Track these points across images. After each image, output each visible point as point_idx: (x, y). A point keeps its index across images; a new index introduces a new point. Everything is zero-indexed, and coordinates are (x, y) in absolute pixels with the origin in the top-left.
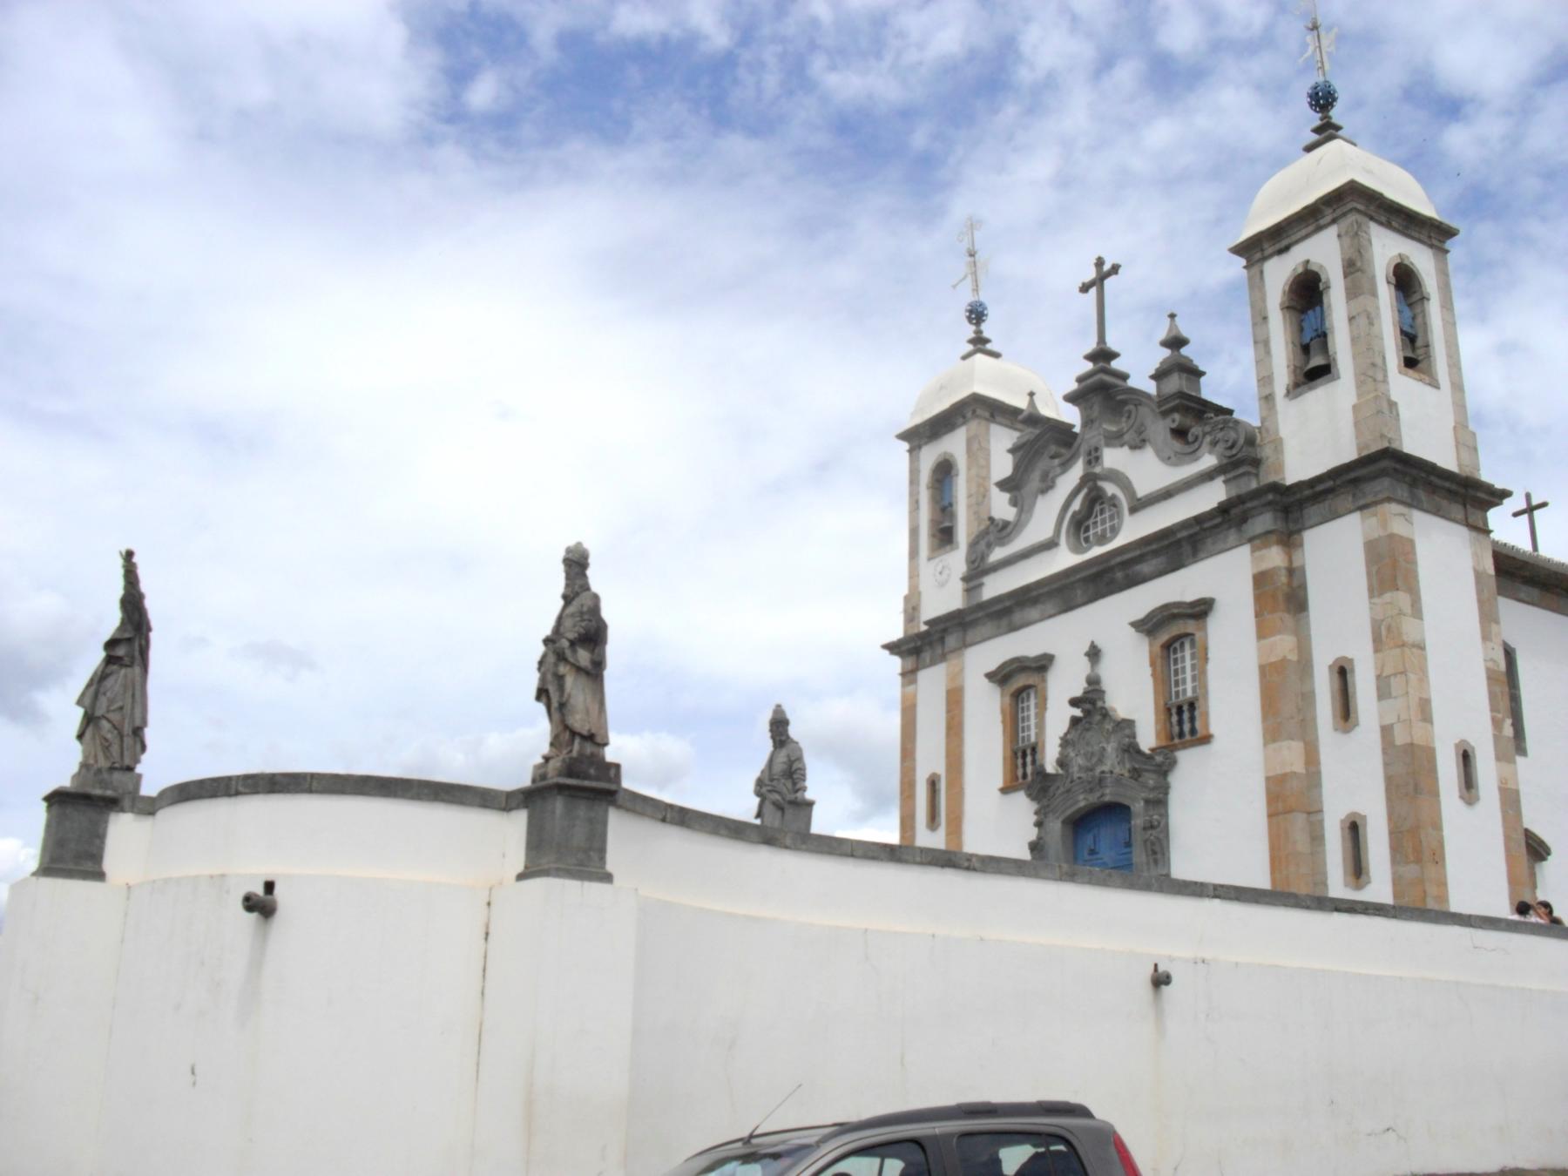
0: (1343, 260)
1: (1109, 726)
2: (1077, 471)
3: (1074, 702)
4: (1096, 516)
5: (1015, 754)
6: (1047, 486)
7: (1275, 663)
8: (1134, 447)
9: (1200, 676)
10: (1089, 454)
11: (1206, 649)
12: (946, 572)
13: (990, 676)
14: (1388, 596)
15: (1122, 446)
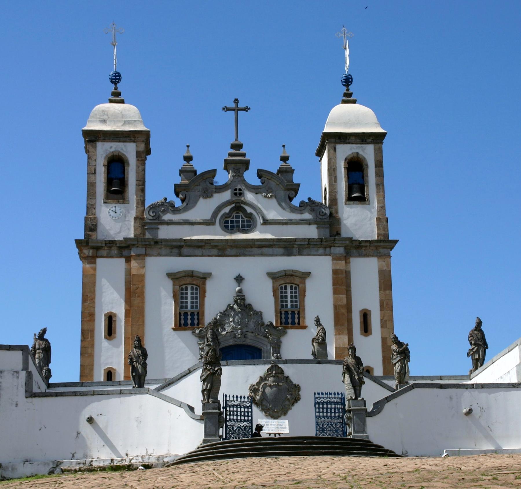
2: (227, 195)
4: (233, 218)
5: (180, 313)
6: (207, 194)
7: (341, 305)
10: (236, 190)
11: (304, 291)
13: (169, 275)
14: (387, 292)
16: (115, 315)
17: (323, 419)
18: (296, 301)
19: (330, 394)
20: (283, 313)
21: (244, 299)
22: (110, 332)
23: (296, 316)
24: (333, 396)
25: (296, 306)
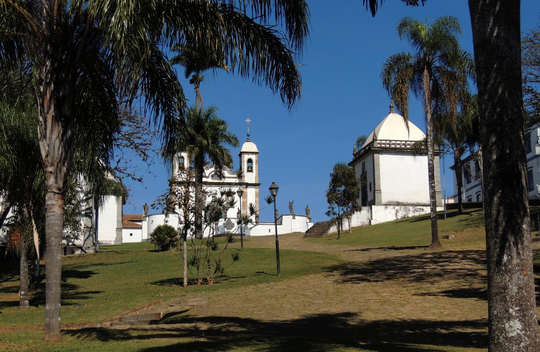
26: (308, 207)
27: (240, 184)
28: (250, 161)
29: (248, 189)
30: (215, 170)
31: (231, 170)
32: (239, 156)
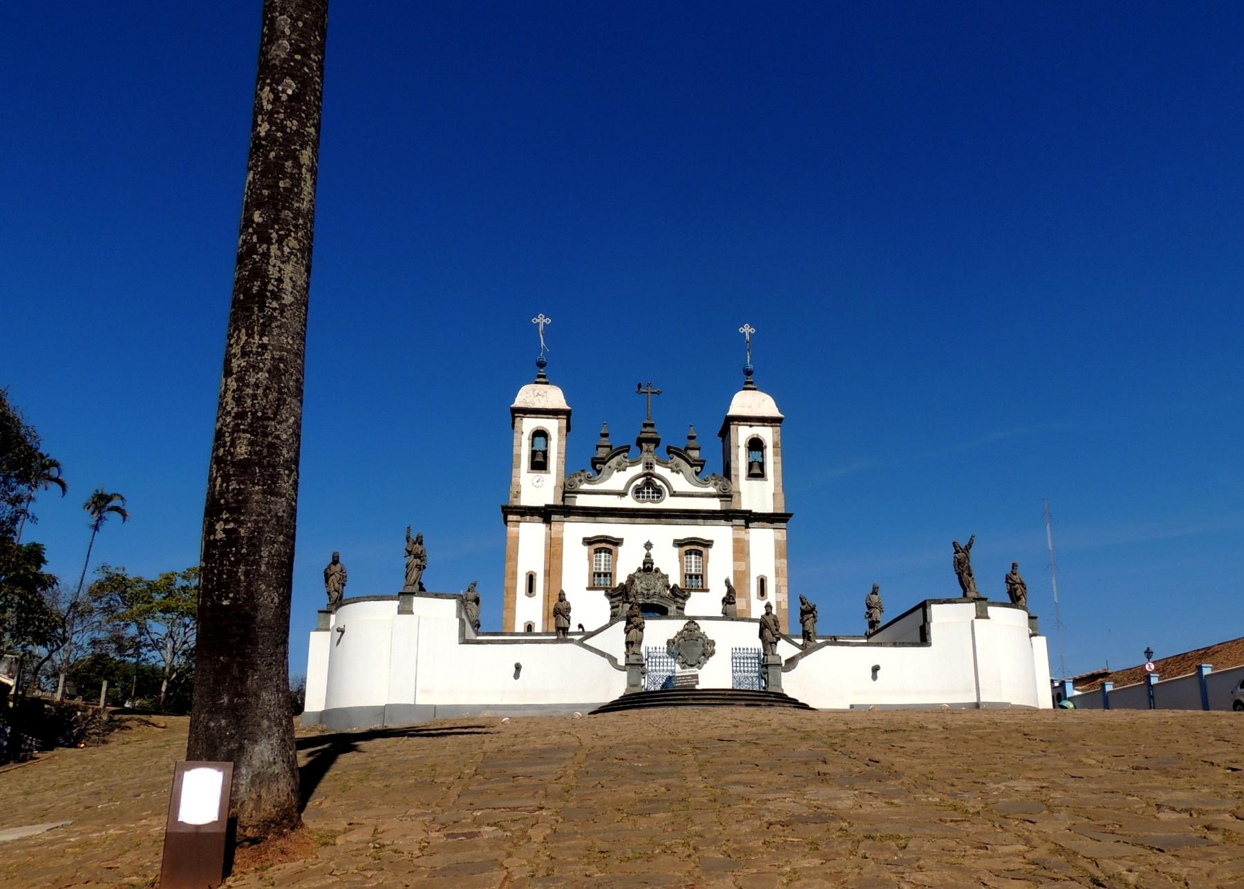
0: (773, 442)
1: (658, 574)
2: (639, 469)
3: (644, 563)
6: (620, 468)
8: (673, 471)
9: (704, 567)
10: (647, 464)
12: (540, 483)
13: (584, 539)
14: (782, 560)
15: (666, 467)
16: (536, 574)
17: (740, 673)
18: (700, 567)
19: (747, 649)
20: (688, 577)
21: (652, 564)
22: (531, 589)
23: (700, 580)
24: (750, 651)
25: (700, 571)
26: (1019, 570)
27: (727, 515)
28: (756, 445)
29: (751, 530)
30: (646, 471)
31: (697, 473)
32: (720, 435)
